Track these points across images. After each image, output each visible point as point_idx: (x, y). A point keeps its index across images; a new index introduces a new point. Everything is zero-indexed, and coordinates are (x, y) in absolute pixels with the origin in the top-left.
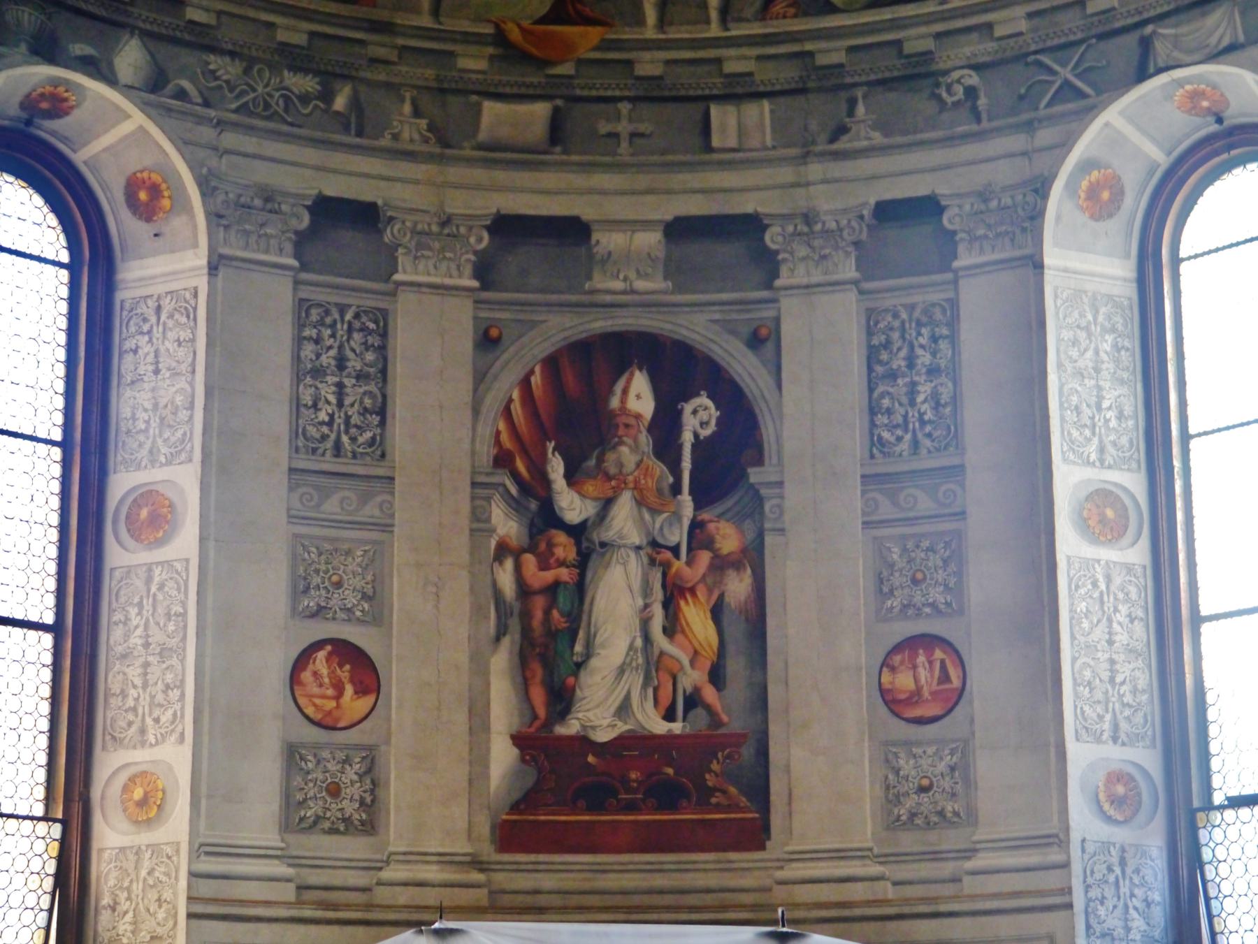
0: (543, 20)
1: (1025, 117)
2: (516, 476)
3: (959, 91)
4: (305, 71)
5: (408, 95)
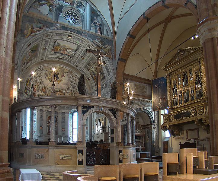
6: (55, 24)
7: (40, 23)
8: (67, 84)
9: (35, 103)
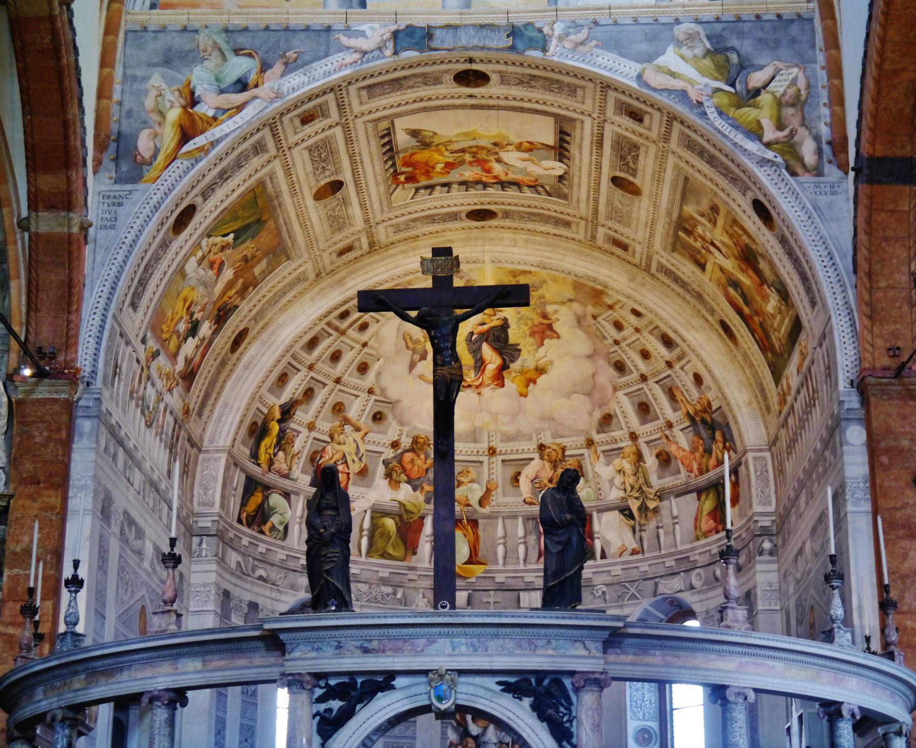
0: (465, 563)
1: (621, 603)
2: (457, 721)
3: (600, 592)
4: (388, 585)
5: (421, 591)
6: (347, 30)
7: (237, 52)
8: (590, 391)
9: (78, 686)
